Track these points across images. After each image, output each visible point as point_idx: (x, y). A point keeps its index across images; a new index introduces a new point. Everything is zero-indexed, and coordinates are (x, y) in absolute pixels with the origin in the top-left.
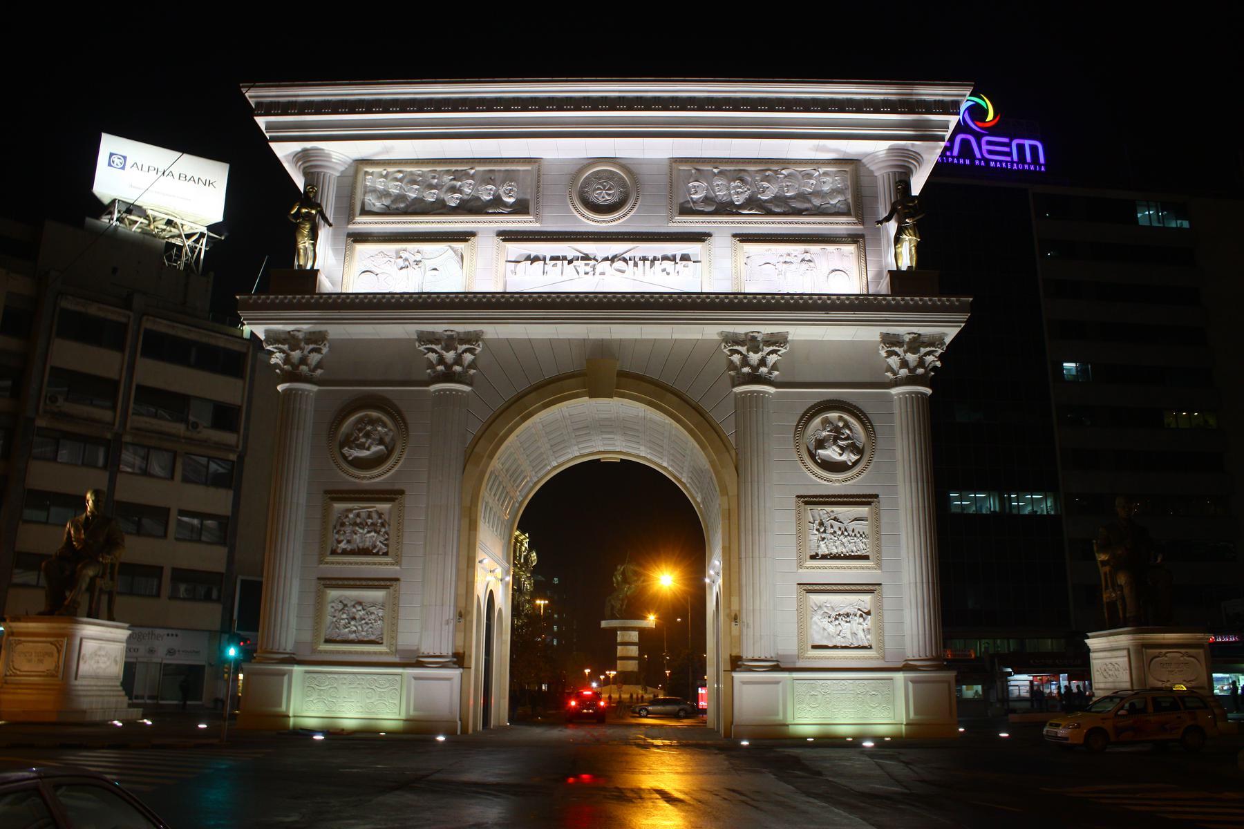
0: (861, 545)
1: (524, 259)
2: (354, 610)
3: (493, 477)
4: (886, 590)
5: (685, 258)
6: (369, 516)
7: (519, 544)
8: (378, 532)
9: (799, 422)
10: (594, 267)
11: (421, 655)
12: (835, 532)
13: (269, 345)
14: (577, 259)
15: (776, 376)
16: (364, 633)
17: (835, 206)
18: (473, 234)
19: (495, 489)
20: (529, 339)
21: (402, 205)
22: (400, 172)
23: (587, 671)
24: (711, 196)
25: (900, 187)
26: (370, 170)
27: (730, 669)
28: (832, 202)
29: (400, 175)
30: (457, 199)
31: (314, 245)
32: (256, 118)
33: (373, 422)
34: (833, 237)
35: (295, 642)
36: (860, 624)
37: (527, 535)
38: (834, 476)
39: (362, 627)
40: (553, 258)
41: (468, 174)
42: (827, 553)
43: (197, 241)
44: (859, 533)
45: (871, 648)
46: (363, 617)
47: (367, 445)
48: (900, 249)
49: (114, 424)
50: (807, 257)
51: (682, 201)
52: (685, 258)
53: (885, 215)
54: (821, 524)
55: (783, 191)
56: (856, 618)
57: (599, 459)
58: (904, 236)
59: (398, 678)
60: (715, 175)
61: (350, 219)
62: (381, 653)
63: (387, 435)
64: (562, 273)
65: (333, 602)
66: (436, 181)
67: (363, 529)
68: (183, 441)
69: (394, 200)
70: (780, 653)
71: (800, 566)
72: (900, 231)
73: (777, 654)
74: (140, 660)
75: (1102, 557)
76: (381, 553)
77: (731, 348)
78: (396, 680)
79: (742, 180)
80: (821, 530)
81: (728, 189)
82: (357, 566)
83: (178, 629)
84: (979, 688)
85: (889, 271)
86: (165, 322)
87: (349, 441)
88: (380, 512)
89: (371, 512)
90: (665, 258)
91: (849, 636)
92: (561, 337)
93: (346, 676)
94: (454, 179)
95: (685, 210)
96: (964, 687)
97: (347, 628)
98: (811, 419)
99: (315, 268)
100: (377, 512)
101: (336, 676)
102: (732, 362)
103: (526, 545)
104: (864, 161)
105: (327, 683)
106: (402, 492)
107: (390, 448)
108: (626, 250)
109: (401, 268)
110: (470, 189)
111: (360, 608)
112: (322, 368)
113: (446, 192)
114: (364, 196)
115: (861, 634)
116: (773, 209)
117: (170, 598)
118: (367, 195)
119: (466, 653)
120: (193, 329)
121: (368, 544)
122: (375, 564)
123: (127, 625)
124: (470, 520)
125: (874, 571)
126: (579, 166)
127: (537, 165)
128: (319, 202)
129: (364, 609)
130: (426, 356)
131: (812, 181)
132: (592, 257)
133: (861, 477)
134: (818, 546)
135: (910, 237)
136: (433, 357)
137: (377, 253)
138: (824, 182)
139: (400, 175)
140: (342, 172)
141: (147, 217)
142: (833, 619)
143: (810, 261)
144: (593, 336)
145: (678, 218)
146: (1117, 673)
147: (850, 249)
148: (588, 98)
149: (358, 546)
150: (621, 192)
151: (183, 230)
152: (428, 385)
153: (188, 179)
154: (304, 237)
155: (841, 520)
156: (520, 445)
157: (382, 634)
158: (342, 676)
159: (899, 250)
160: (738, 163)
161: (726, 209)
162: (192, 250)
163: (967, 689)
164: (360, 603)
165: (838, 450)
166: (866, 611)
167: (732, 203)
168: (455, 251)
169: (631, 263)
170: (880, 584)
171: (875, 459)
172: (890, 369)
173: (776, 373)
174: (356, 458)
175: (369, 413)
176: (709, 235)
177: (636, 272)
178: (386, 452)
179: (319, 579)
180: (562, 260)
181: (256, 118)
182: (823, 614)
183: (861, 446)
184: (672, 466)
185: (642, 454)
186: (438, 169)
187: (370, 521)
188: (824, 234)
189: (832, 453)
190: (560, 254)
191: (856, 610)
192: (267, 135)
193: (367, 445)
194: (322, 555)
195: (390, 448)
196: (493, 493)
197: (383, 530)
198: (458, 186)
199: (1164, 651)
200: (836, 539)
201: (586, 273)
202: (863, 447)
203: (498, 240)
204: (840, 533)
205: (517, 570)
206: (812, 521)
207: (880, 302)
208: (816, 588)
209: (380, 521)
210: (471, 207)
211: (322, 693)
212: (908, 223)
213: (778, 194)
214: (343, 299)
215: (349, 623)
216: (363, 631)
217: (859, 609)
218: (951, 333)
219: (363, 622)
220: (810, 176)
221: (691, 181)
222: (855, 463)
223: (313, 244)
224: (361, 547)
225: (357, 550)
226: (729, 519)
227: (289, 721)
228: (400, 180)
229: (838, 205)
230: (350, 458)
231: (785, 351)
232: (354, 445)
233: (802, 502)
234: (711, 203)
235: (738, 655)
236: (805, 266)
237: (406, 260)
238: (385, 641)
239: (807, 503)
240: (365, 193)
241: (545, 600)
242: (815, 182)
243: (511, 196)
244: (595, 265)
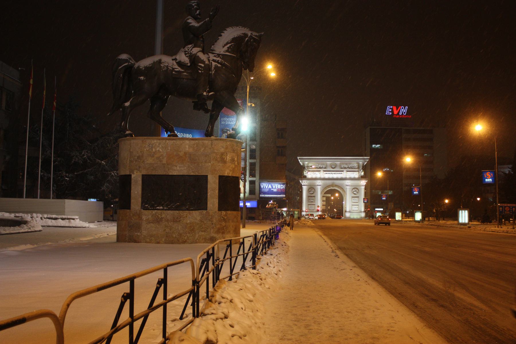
18: (320, 171)
33: (312, 190)
52: (341, 173)
61: (308, 169)
72: (362, 171)
87: (310, 192)
95: (341, 168)
106: (315, 196)
147: (357, 172)
161: (345, 168)
167: (346, 167)
189: (355, 193)
210: (320, 168)
218: (366, 182)
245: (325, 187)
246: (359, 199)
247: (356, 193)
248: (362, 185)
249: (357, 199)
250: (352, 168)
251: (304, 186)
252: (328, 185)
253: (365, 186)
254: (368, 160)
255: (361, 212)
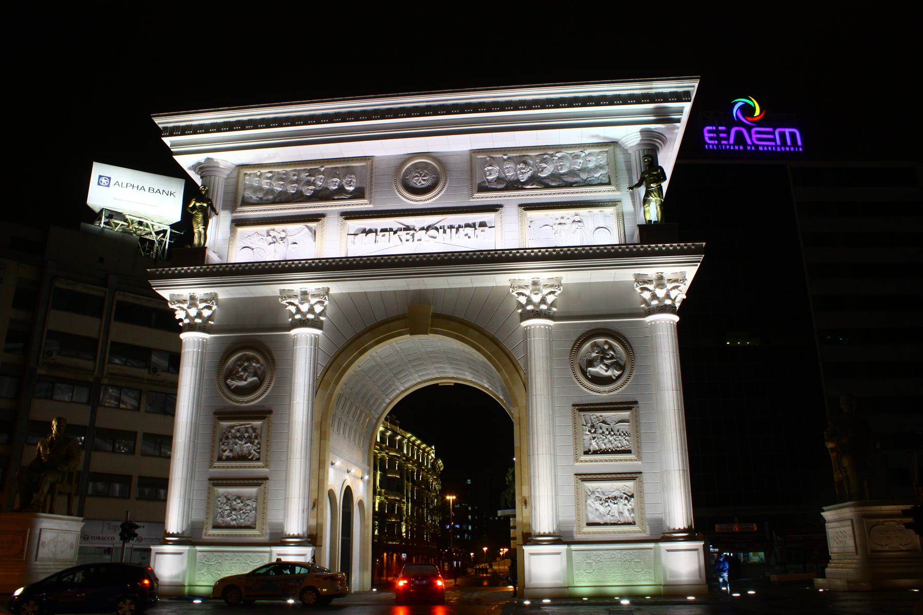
0: (625, 442)
1: (361, 232)
2: (235, 503)
3: (343, 400)
4: (645, 477)
5: (483, 224)
6: (247, 431)
7: (426, 454)
8: (252, 443)
9: (573, 347)
10: (413, 235)
11: (284, 536)
12: (603, 432)
13: (172, 305)
14: (401, 230)
15: (554, 312)
16: (242, 521)
17: (598, 178)
18: (323, 215)
19: (347, 408)
20: (365, 292)
21: (271, 197)
22: (270, 172)
23: (485, 549)
24: (502, 177)
25: (646, 160)
26: (249, 172)
27: (521, 543)
28: (595, 176)
29: (270, 175)
30: (311, 190)
31: (205, 229)
32: (163, 138)
33: (249, 359)
34: (597, 202)
35: (192, 528)
36: (625, 505)
37: (433, 447)
38: (602, 388)
39: (240, 516)
40: (383, 230)
41: (320, 171)
42: (597, 448)
43: (164, 236)
44: (623, 432)
45: (635, 524)
46: (242, 508)
47: (244, 377)
48: (648, 208)
49: (94, 371)
50: (577, 218)
51: (480, 182)
52: (483, 224)
53: (637, 182)
54: (593, 426)
55: (558, 170)
56: (622, 500)
57: (438, 384)
58: (651, 198)
59: (267, 555)
60: (505, 160)
62: (254, 536)
63: (260, 369)
64: (389, 241)
65: (220, 497)
66: (296, 177)
67: (241, 441)
68: (146, 382)
69: (266, 193)
70: (562, 530)
71: (577, 460)
72: (648, 193)
73: (560, 530)
74: (116, 545)
75: (830, 445)
76: (254, 459)
77: (517, 291)
78: (265, 556)
79: (525, 163)
80: (592, 431)
81: (515, 170)
82: (236, 470)
83: (144, 522)
84: (762, 554)
85: (638, 225)
86: (132, 295)
87: (232, 374)
88: (255, 427)
89: (248, 428)
90: (467, 226)
91: (617, 515)
92: (388, 289)
93: (228, 554)
94: (310, 175)
95: (483, 189)
96: (751, 554)
97: (229, 517)
98: (583, 344)
99: (206, 246)
100: (252, 427)
101: (221, 554)
102: (520, 303)
103: (433, 455)
104: (619, 142)
105: (214, 560)
106: (270, 412)
107: (262, 379)
108: (439, 220)
109: (270, 244)
110: (321, 182)
111: (239, 501)
112: (212, 321)
113: (304, 185)
114: (244, 192)
115: (626, 514)
116: (550, 184)
117: (137, 499)
118: (246, 191)
119: (319, 535)
120: (152, 299)
121: (245, 451)
122: (250, 467)
123: (81, 519)
124: (321, 431)
125: (635, 462)
126: (403, 160)
127: (369, 162)
128: (211, 198)
129: (242, 502)
130: (287, 308)
131: (579, 161)
132: (412, 228)
133: (625, 386)
134: (590, 444)
135: (656, 198)
136: (293, 309)
137: (253, 233)
138: (589, 161)
139: (270, 175)
140: (228, 175)
141: (126, 220)
142: (604, 502)
143: (579, 221)
144: (412, 288)
145: (477, 195)
146: (845, 539)
148: (404, 108)
149: (238, 454)
150: (433, 178)
151: (153, 229)
152: (289, 330)
153: (155, 191)
154: (198, 223)
155: (608, 422)
156: (364, 374)
157: (255, 521)
158: (225, 554)
159: (647, 209)
160: (522, 150)
161: (514, 185)
162: (160, 242)
163: (754, 555)
164: (239, 497)
165: (604, 367)
166: (630, 494)
167: (518, 181)
168: (310, 229)
169: (441, 231)
170: (641, 473)
171: (634, 374)
172: (645, 301)
173: (554, 309)
174: (237, 387)
175: (247, 353)
176: (501, 206)
177: (445, 237)
178: (259, 382)
179: (210, 479)
180: (389, 232)
181: (163, 138)
182: (595, 498)
183: (623, 364)
184: (490, 386)
185: (469, 378)
186: (298, 168)
187: (246, 435)
188: (592, 200)
189: (600, 370)
190: (388, 227)
191: (622, 494)
192: (172, 150)
193: (244, 377)
194: (212, 461)
195: (262, 379)
196: (345, 412)
197: (256, 441)
198: (312, 181)
199: (882, 520)
200: (605, 437)
201: (407, 240)
202: (625, 364)
203: (341, 218)
204: (607, 433)
205: (425, 474)
206: (585, 424)
207: (631, 250)
208: (589, 477)
209: (254, 434)
210: (322, 195)
211: (210, 567)
212: (653, 187)
213: (554, 172)
214: (237, 267)
215: (231, 513)
216: (241, 519)
217: (625, 493)
218: (691, 272)
219: (242, 512)
220: (577, 156)
221: (487, 165)
222: (619, 377)
223: (204, 229)
224: (240, 455)
225: (237, 457)
226: (520, 425)
227: (185, 589)
228: (270, 178)
229: (601, 177)
230: (233, 387)
231: (561, 292)
232: (235, 378)
233: (577, 409)
234: (501, 181)
235: (529, 532)
236: (575, 225)
237: (274, 237)
238: (257, 527)
239: (580, 410)
240: (245, 190)
241: (453, 495)
242: (582, 161)
243: (350, 186)
244: (414, 234)
245: (350, 335)
246: (636, 422)
247: (613, 373)
248: (655, 303)
249: (624, 427)
250: (560, 181)
251: (192, 327)
252: (381, 317)
253: (686, 310)
254: (687, 106)
255: (668, 537)
